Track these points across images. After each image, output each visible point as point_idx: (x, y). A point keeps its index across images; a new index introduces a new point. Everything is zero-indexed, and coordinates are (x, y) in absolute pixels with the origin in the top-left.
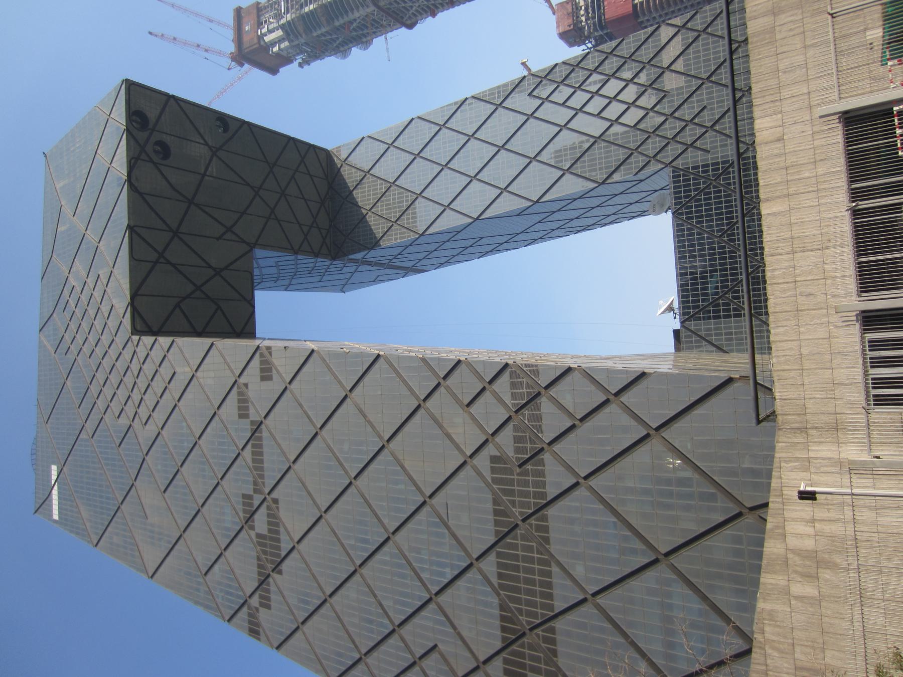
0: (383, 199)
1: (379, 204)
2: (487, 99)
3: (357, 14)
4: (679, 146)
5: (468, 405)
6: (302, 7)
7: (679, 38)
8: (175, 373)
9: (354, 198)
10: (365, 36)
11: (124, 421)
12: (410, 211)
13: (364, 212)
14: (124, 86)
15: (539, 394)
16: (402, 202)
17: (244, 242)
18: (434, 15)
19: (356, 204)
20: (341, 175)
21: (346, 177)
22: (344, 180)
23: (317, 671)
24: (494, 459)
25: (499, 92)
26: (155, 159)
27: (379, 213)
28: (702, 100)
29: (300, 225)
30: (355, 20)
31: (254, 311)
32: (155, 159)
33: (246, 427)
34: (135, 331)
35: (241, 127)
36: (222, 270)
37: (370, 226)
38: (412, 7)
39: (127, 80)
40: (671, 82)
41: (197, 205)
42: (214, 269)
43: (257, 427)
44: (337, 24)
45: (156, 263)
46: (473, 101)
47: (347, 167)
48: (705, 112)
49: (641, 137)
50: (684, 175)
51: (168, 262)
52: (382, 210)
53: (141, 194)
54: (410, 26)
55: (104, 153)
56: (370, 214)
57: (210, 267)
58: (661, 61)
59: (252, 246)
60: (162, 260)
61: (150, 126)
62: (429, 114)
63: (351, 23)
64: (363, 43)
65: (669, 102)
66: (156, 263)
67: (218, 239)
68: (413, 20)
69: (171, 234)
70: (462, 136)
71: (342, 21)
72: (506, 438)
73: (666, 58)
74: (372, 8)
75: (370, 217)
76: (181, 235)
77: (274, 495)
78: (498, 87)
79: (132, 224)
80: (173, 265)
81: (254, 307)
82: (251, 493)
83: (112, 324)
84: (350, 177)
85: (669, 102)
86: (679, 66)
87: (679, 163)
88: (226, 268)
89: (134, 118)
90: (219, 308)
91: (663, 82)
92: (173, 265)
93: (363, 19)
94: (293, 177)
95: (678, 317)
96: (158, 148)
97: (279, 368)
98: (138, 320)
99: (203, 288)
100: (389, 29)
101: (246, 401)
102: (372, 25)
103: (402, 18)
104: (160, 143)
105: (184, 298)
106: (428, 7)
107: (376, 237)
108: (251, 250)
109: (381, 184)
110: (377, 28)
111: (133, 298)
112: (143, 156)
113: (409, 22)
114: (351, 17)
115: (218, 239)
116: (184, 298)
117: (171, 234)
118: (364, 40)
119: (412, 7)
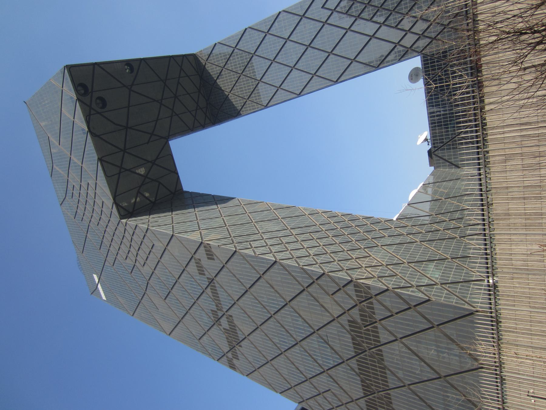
0: (237, 84)
1: (235, 88)
8: (153, 245)
9: (218, 85)
11: (130, 262)
12: (255, 92)
13: (227, 93)
14: (66, 71)
16: (250, 86)
17: (162, 138)
19: (220, 89)
20: (207, 71)
21: (210, 71)
22: (209, 73)
23: (269, 388)
26: (99, 110)
27: (237, 94)
29: (190, 112)
31: (179, 176)
36: (155, 160)
37: (232, 102)
39: (67, 66)
41: (130, 128)
42: (151, 162)
43: (211, 281)
45: (119, 174)
47: (209, 65)
50: (431, 59)
51: (126, 170)
52: (238, 92)
53: (98, 136)
55: (67, 113)
56: (230, 95)
57: (148, 162)
60: (122, 170)
61: (90, 91)
62: (257, 25)
66: (119, 174)
67: (148, 143)
69: (122, 152)
70: (281, 40)
75: (231, 97)
76: (127, 151)
78: (300, 3)
79: (100, 157)
81: (177, 174)
82: (216, 310)
83: (106, 211)
84: (212, 70)
87: (427, 51)
88: (157, 158)
89: (79, 88)
90: (160, 183)
94: (179, 83)
95: (430, 144)
96: (98, 101)
97: (239, 327)
98: (121, 210)
99: (148, 176)
101: (202, 267)
104: (100, 98)
105: (140, 187)
107: (237, 110)
111: (114, 199)
112: (93, 112)
115: (148, 143)
116: (140, 187)
117: (122, 152)
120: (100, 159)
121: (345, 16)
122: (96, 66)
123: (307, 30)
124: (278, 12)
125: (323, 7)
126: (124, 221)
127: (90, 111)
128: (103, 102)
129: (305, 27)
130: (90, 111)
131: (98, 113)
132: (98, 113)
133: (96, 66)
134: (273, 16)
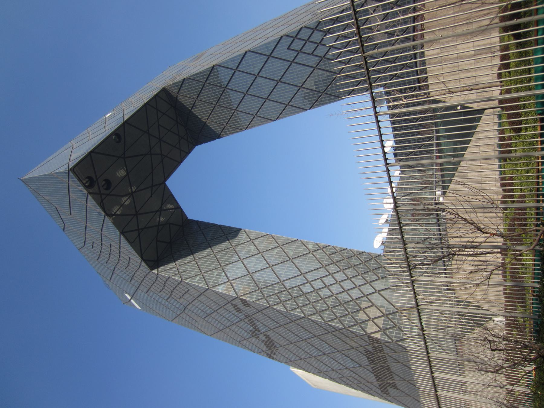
26: (107, 192)
47: (181, 97)
57: (156, 212)
67: (151, 196)
75: (209, 123)
81: (180, 208)
84: (185, 100)
88: (162, 204)
108: (165, 184)
115: (151, 196)
117: (135, 217)
120: (122, 233)
121: (311, 56)
122: (92, 154)
123: (275, 68)
124: (243, 52)
125: (288, 49)
126: (155, 271)
127: (101, 198)
130: (101, 198)
131: (107, 195)
132: (107, 195)
133: (92, 154)
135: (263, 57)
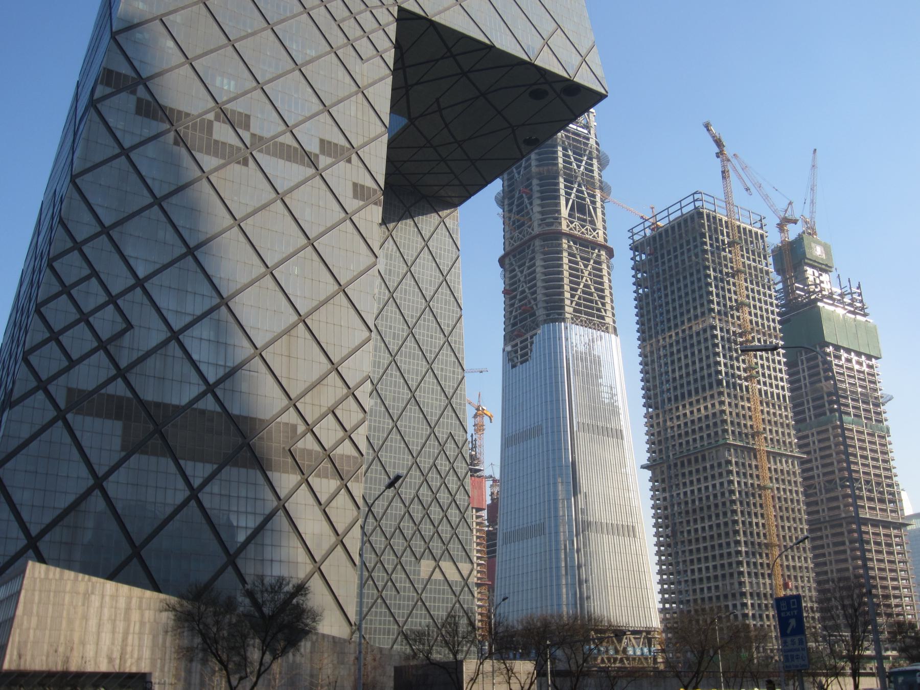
2: (458, 392)
3: (537, 209)
4: (372, 565)
5: (333, 412)
6: (565, 149)
7: (459, 579)
9: (406, 219)
10: (510, 204)
15: (342, 479)
18: (505, 292)
24: (294, 427)
25: (460, 404)
28: (404, 591)
30: (531, 204)
32: (535, 87)
33: (313, 147)
34: (401, 10)
35: (521, 152)
38: (522, 272)
40: (426, 565)
44: (535, 182)
46: (460, 377)
48: (394, 593)
49: (388, 531)
51: (442, 58)
54: (501, 261)
57: (417, 84)
58: (445, 560)
59: (412, 121)
63: (530, 198)
64: (503, 198)
65: (411, 562)
67: (437, 100)
68: (507, 266)
71: (536, 188)
72: (308, 443)
73: (446, 565)
74: (537, 230)
77: (251, 161)
80: (437, 60)
85: (411, 562)
86: (437, 576)
91: (428, 559)
92: (437, 60)
93: (528, 213)
100: (508, 236)
102: (518, 221)
103: (514, 256)
106: (515, 289)
109: (442, 293)
110: (514, 223)
113: (507, 261)
114: (537, 202)
115: (437, 100)
118: (506, 202)
119: (522, 272)
128: (537, 95)
129: (436, 399)
134: (463, 358)
135: (452, 391)
